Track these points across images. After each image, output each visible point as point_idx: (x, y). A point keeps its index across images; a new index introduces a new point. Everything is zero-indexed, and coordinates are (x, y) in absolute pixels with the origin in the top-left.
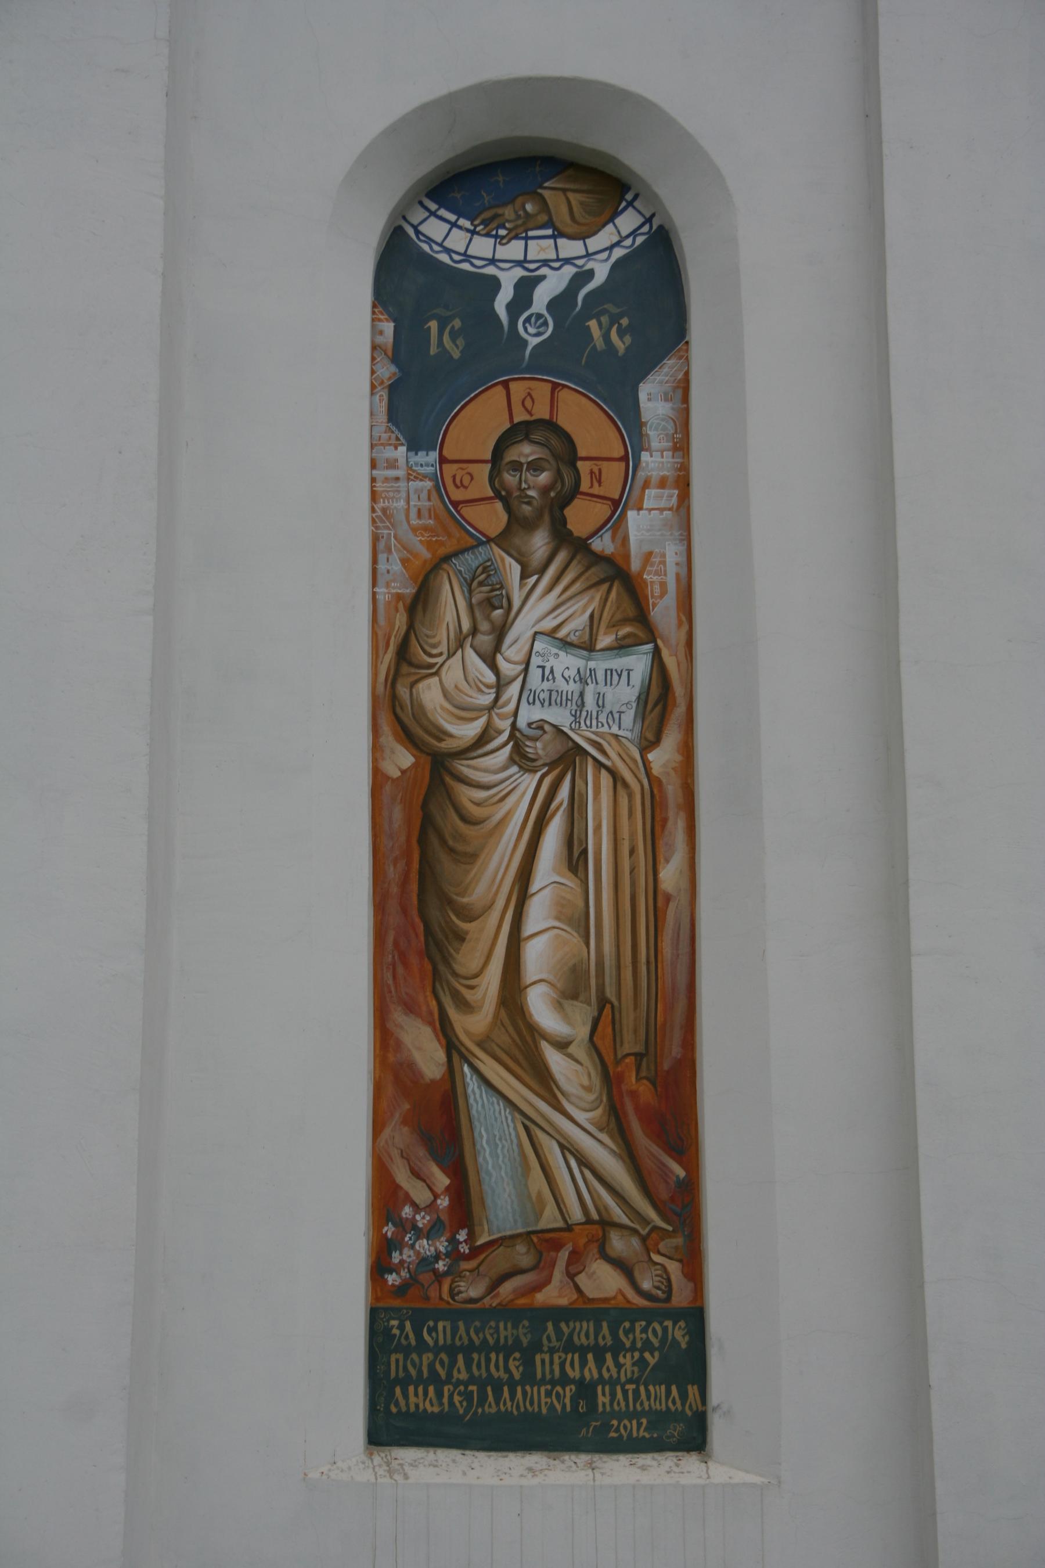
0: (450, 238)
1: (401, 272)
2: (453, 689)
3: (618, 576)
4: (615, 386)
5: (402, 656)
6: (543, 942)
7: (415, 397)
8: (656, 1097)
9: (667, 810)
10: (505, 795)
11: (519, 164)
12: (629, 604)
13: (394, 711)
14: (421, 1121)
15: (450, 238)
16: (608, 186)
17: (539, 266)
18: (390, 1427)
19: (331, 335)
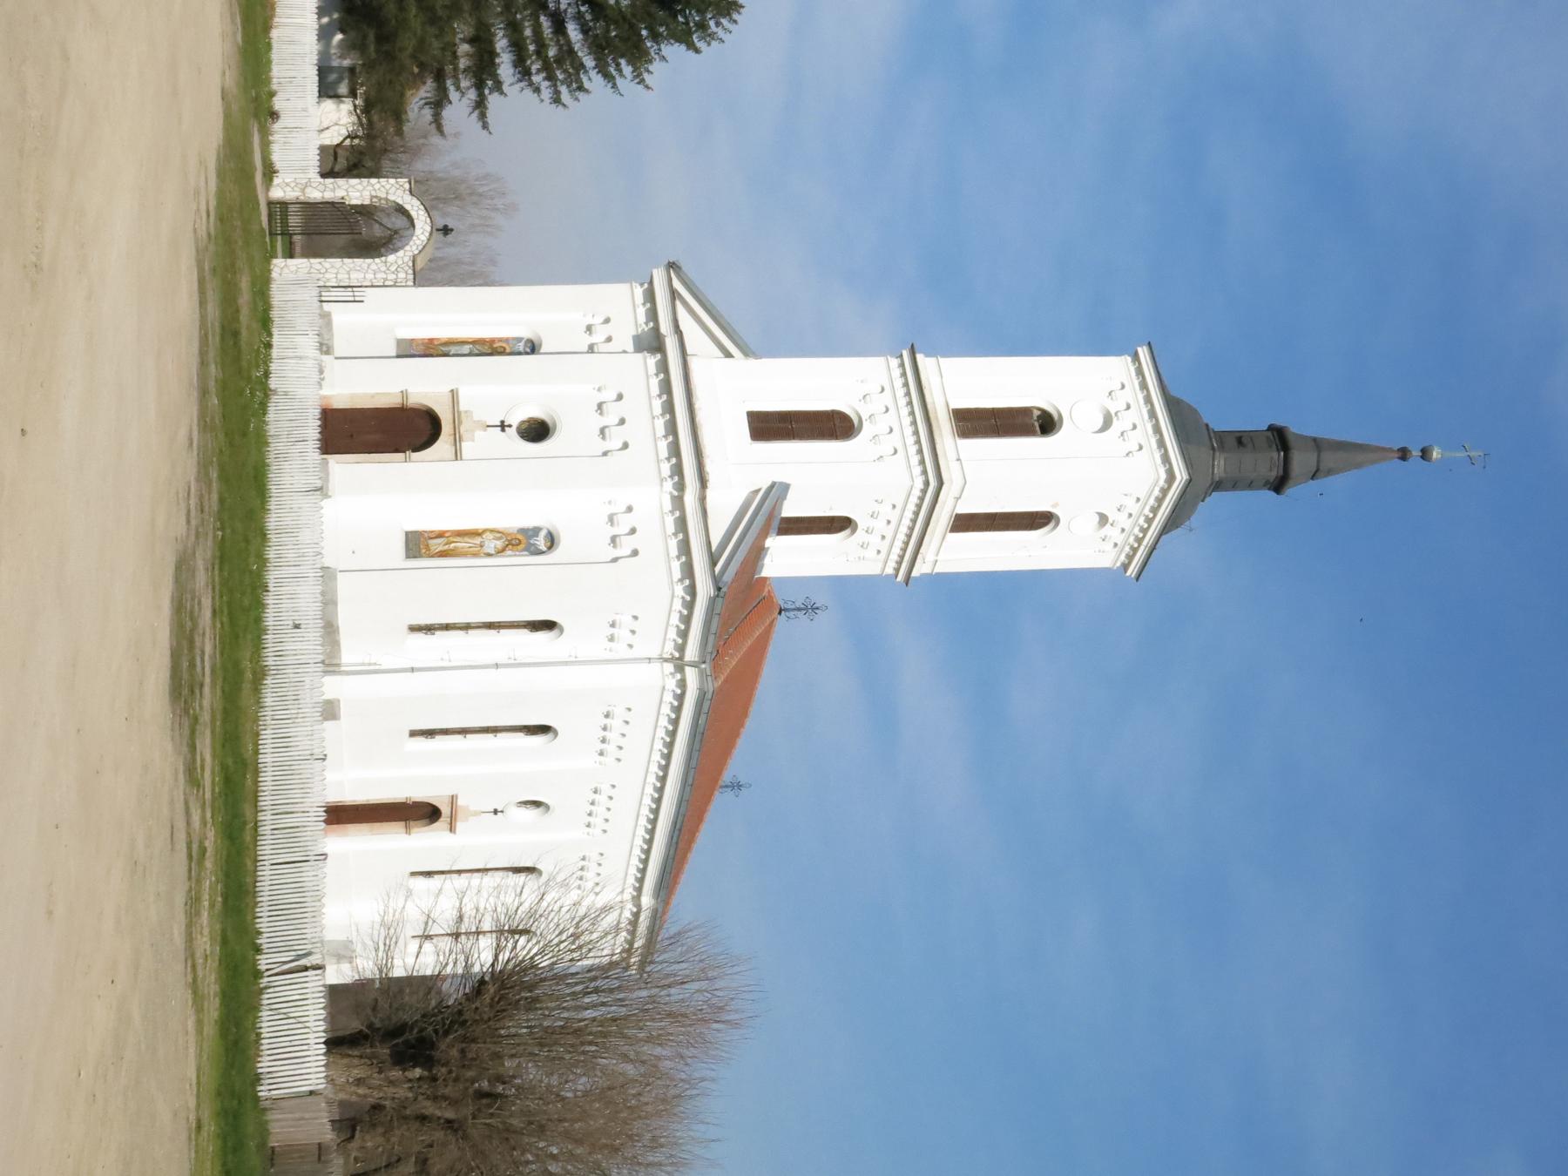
0: (543, 534)
1: (536, 531)
2: (488, 536)
3: (503, 550)
4: (525, 549)
5: (492, 531)
6: (462, 544)
7: (523, 531)
8: (443, 554)
9: (475, 555)
10: (478, 540)
11: (552, 541)
12: (500, 552)
13: (485, 531)
14: (441, 535)
15: (543, 534)
16: (550, 548)
17: (541, 542)
18: (407, 534)
19: (529, 523)
